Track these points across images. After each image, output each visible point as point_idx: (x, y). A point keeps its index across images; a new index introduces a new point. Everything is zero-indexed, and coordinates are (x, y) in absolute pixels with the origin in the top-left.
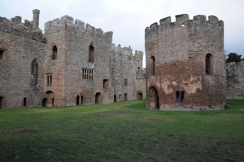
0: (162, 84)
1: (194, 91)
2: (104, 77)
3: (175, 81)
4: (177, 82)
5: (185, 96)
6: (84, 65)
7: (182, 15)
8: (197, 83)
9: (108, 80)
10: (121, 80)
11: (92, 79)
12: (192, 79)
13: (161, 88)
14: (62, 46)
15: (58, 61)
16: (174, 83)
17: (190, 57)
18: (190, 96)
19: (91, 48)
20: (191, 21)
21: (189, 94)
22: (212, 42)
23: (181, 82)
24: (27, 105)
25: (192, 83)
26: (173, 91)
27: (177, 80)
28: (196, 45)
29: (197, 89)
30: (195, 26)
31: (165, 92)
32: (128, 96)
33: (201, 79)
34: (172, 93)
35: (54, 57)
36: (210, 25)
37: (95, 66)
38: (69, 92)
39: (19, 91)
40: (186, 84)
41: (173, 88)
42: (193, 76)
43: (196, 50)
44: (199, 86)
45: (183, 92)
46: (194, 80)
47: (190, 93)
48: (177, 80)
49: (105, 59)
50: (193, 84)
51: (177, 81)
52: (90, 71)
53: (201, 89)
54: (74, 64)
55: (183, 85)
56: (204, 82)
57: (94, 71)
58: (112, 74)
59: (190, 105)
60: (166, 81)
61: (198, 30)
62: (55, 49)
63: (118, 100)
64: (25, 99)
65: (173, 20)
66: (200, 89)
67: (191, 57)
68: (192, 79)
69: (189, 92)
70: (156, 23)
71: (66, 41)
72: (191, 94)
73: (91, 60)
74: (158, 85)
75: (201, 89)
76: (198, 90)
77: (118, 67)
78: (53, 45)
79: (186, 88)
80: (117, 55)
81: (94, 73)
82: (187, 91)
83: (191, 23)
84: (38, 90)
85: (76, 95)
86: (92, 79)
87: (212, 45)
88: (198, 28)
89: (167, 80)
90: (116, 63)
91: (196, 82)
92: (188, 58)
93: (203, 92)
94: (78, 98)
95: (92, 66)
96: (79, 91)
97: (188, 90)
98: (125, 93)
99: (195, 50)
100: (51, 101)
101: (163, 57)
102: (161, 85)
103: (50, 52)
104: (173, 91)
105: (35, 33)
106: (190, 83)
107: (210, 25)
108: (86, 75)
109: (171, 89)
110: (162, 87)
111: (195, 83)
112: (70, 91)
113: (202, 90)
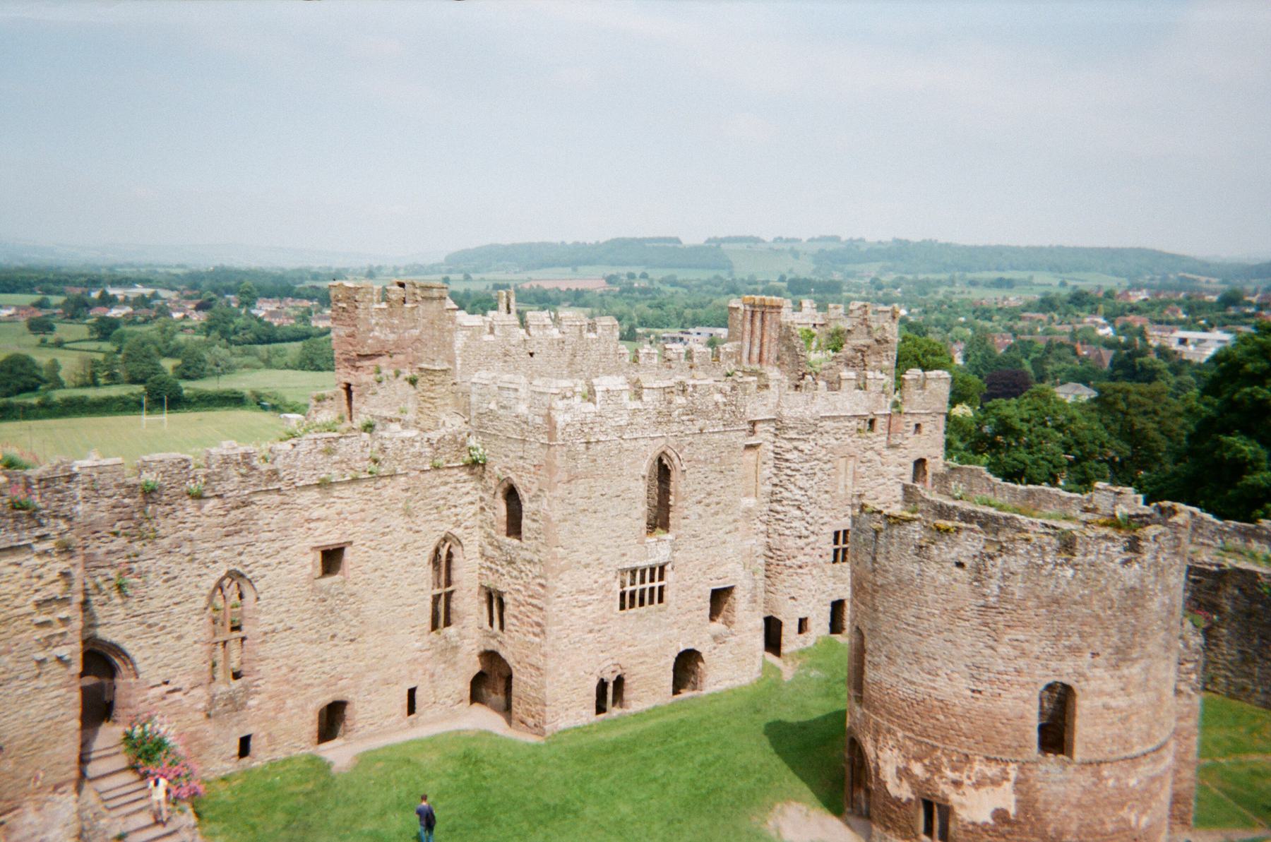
0: (880, 754)
2: (715, 581)
5: (952, 825)
6: (624, 559)
8: (999, 790)
9: (732, 588)
10: (808, 550)
11: (661, 600)
15: (525, 543)
16: (917, 769)
18: (971, 832)
19: (663, 472)
22: (1075, 639)
23: (939, 770)
24: (417, 710)
25: (978, 785)
26: (913, 797)
30: (1004, 578)
34: (909, 800)
38: (568, 674)
39: (392, 670)
40: (957, 784)
41: (912, 785)
44: (1005, 798)
45: (947, 811)
47: (968, 820)
48: (927, 762)
49: (718, 503)
50: (983, 790)
51: (925, 765)
52: (652, 570)
53: (1012, 811)
54: (587, 566)
57: (668, 568)
58: (768, 523)
61: (1013, 594)
63: (791, 640)
64: (412, 692)
66: (1005, 812)
67: (980, 692)
72: (974, 824)
73: (659, 519)
76: (1000, 815)
77: (796, 491)
78: (506, 485)
80: (792, 434)
81: (669, 575)
82: (957, 810)
84: (455, 648)
85: (594, 683)
86: (661, 600)
87: (1075, 650)
88: (1017, 588)
91: (995, 783)
92: (970, 693)
93: (1018, 822)
94: (602, 686)
95: (658, 549)
96: (610, 662)
97: (962, 806)
98: (836, 598)
99: (996, 668)
100: (501, 686)
102: (877, 757)
104: (914, 793)
105: (439, 441)
108: (632, 594)
109: (906, 785)
110: (881, 764)
111: (989, 788)
112: (572, 669)
113: (1017, 815)
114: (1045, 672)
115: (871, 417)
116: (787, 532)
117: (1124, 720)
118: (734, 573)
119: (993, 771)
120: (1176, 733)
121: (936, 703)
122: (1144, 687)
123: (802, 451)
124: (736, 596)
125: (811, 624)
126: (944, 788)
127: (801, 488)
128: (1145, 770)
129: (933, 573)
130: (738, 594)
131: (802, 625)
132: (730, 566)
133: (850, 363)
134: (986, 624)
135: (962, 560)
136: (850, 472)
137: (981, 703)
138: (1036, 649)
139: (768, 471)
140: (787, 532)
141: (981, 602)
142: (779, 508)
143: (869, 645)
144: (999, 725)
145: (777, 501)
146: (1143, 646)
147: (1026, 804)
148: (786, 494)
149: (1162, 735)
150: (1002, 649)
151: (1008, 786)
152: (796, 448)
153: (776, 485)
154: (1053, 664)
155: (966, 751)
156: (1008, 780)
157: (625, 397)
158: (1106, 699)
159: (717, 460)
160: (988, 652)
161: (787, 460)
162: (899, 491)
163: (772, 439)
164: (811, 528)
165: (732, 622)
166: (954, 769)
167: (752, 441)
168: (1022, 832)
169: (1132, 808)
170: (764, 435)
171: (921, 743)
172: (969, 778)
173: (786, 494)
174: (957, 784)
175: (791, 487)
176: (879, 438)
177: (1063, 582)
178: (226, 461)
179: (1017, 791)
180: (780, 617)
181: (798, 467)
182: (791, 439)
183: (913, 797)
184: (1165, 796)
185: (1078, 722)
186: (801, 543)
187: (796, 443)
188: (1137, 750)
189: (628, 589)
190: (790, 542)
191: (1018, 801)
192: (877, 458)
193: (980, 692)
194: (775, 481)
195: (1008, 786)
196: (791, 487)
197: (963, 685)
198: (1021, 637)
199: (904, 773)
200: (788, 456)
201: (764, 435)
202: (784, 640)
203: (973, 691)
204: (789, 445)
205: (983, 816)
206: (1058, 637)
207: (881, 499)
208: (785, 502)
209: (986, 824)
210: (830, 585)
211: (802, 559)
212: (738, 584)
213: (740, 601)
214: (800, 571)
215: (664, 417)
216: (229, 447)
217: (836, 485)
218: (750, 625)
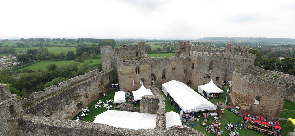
14: (196, 66)
16: (237, 102)
25: (245, 105)
28: (251, 90)
30: (253, 81)
35: (193, 68)
36: (264, 82)
37: (212, 72)
62: (193, 64)
68: (245, 104)
71: (198, 64)
73: (210, 69)
88: (255, 83)
91: (247, 106)
95: (210, 72)
103: (191, 66)
107: (264, 82)
118: (219, 75)
120: (279, 105)
122: (274, 99)
128: (272, 109)
130: (220, 78)
133: (242, 52)
143: (233, 87)
146: (275, 93)
149: (275, 105)
157: (207, 54)
158: (266, 99)
162: (246, 68)
169: (268, 113)
174: (242, 105)
176: (244, 62)
177: (262, 83)
178: (164, 58)
184: (275, 112)
188: (270, 106)
189: (206, 76)
197: (245, 93)
199: (235, 102)
206: (260, 90)
213: (220, 79)
215: (212, 57)
216: (165, 57)
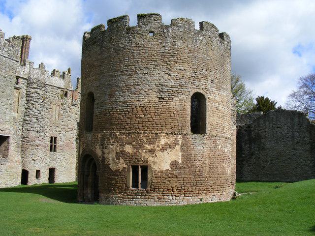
1: (166, 166)
3: (130, 143)
4: (134, 147)
5: (149, 176)
7: (150, 15)
9: (8, 137)
10: (40, 138)
12: (163, 141)
13: (104, 157)
16: (128, 149)
17: (161, 98)
20: (167, 27)
21: (157, 172)
25: (163, 149)
26: (126, 167)
27: (134, 143)
29: (173, 162)
31: (111, 166)
32: (57, 173)
33: (180, 142)
40: (152, 151)
42: (164, 136)
43: (172, 84)
44: (176, 155)
45: (145, 169)
46: (166, 144)
47: (158, 170)
48: (134, 143)
50: (165, 152)
51: (133, 146)
53: (180, 161)
55: (146, 152)
56: (185, 148)
59: (158, 194)
60: (112, 145)
65: (133, 22)
67: (163, 98)
68: (163, 141)
69: (156, 168)
70: (100, 26)
72: (161, 172)
74: (99, 152)
75: (180, 161)
76: (174, 164)
77: (36, 111)
79: (151, 159)
80: (35, 86)
83: (165, 31)
87: (205, 78)
89: (114, 142)
90: (33, 102)
91: (171, 147)
92: (157, 99)
97: (154, 163)
99: (170, 84)
101: (109, 95)
102: (104, 153)
106: (159, 149)
107: (201, 38)
109: (122, 160)
110: (106, 156)
111: (169, 150)
114: (193, 87)
115: (66, 90)
116: (32, 129)
117: (223, 117)
119: (170, 140)
121: (139, 109)
123: (39, 94)
124: (10, 142)
125: (41, 174)
126: (144, 154)
127: (38, 110)
129: (137, 39)
130: (11, 141)
131: (38, 172)
132: (7, 126)
134: (165, 62)
135: (153, 30)
136: (57, 112)
137: (164, 104)
138: (189, 74)
139: (23, 101)
140: (32, 129)
141: (162, 50)
142: (28, 119)
144: (172, 115)
145: (27, 115)
147: (187, 156)
148: (31, 112)
150: (173, 74)
151: (178, 147)
152: (36, 92)
153: (26, 109)
154: (197, 83)
155: (156, 132)
156: (178, 144)
159: (3, 71)
160: (166, 76)
161: (32, 97)
163: (26, 88)
164: (42, 129)
165: (7, 156)
166: (150, 144)
167: (17, 86)
168: (185, 173)
170: (22, 85)
171: (129, 134)
172: (158, 146)
173: (31, 112)
174: (152, 151)
175: (34, 109)
179: (182, 150)
180: (27, 169)
181: (36, 100)
182: (34, 88)
183: (126, 167)
185: (207, 113)
186: (38, 135)
187: (36, 90)
190: (33, 133)
191: (182, 156)
192: (68, 109)
193: (163, 98)
194: (26, 107)
195: (178, 147)
196: (34, 109)
197: (154, 96)
198: (182, 68)
200: (33, 95)
201: (22, 84)
202: (29, 180)
203: (160, 98)
204: (33, 90)
205: (166, 166)
207: (70, 127)
208: (30, 116)
209: (167, 170)
210: (49, 160)
211: (38, 142)
212: (11, 136)
214: (37, 147)
217: (52, 116)
218: (16, 159)
